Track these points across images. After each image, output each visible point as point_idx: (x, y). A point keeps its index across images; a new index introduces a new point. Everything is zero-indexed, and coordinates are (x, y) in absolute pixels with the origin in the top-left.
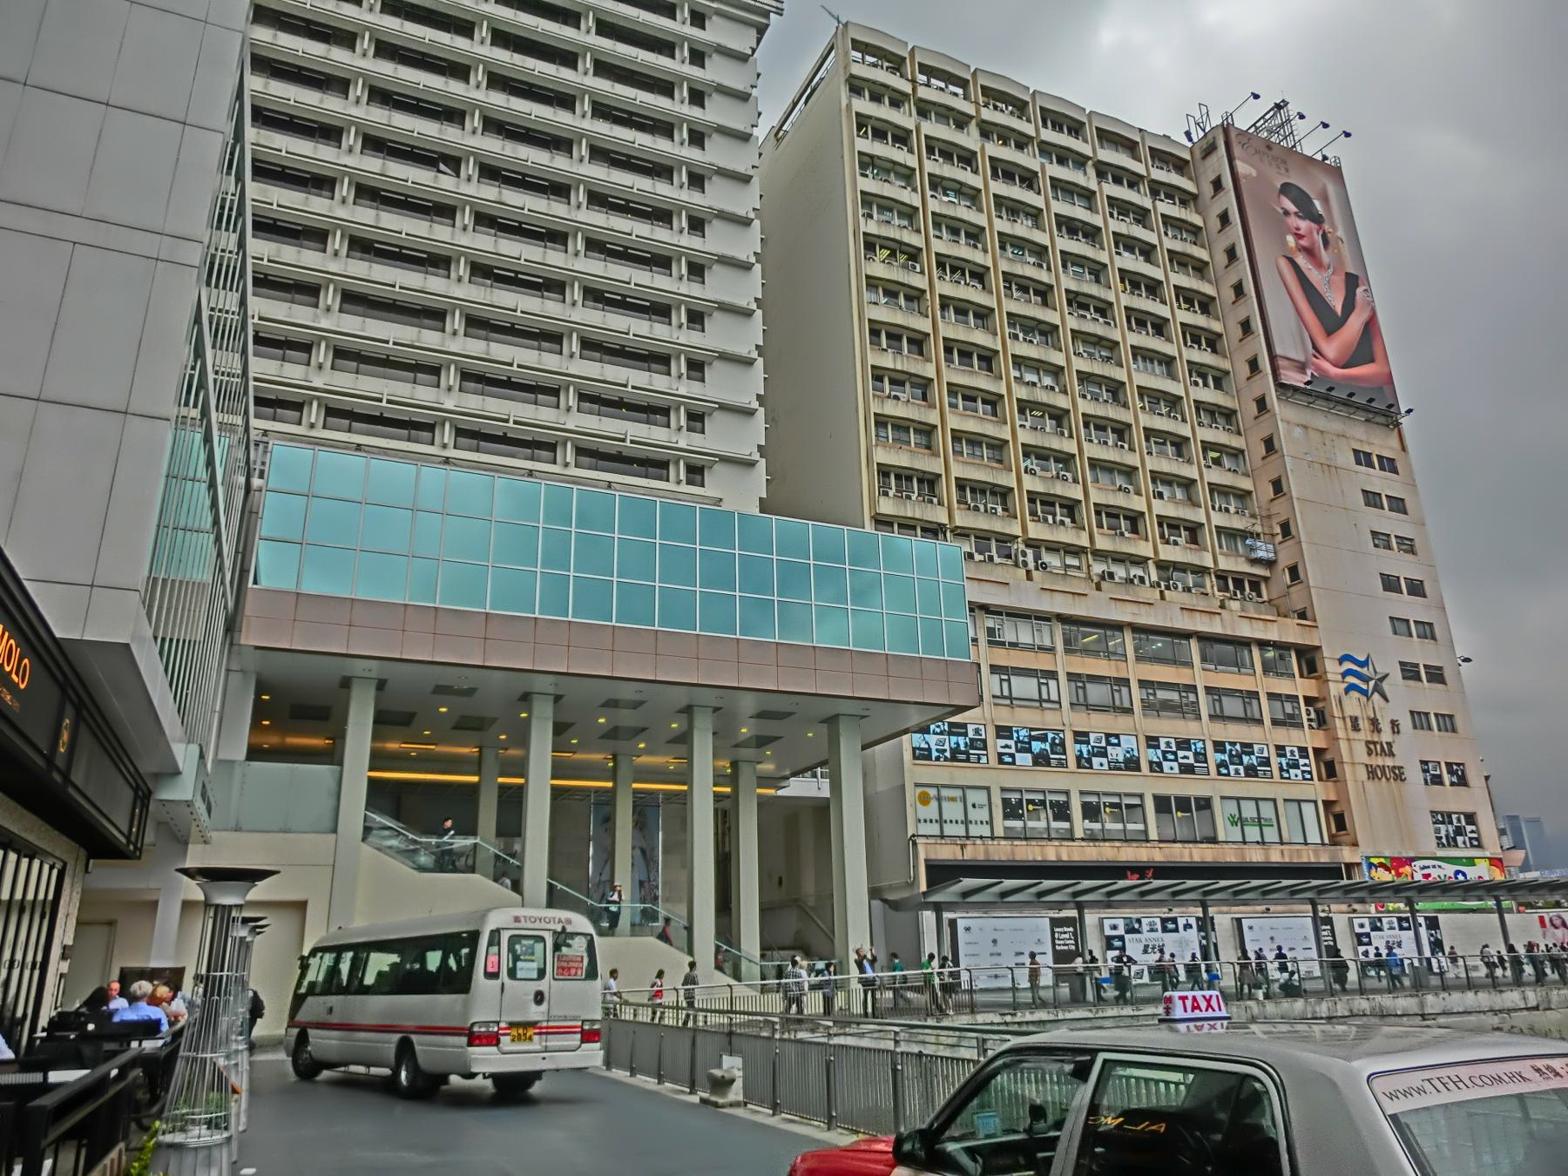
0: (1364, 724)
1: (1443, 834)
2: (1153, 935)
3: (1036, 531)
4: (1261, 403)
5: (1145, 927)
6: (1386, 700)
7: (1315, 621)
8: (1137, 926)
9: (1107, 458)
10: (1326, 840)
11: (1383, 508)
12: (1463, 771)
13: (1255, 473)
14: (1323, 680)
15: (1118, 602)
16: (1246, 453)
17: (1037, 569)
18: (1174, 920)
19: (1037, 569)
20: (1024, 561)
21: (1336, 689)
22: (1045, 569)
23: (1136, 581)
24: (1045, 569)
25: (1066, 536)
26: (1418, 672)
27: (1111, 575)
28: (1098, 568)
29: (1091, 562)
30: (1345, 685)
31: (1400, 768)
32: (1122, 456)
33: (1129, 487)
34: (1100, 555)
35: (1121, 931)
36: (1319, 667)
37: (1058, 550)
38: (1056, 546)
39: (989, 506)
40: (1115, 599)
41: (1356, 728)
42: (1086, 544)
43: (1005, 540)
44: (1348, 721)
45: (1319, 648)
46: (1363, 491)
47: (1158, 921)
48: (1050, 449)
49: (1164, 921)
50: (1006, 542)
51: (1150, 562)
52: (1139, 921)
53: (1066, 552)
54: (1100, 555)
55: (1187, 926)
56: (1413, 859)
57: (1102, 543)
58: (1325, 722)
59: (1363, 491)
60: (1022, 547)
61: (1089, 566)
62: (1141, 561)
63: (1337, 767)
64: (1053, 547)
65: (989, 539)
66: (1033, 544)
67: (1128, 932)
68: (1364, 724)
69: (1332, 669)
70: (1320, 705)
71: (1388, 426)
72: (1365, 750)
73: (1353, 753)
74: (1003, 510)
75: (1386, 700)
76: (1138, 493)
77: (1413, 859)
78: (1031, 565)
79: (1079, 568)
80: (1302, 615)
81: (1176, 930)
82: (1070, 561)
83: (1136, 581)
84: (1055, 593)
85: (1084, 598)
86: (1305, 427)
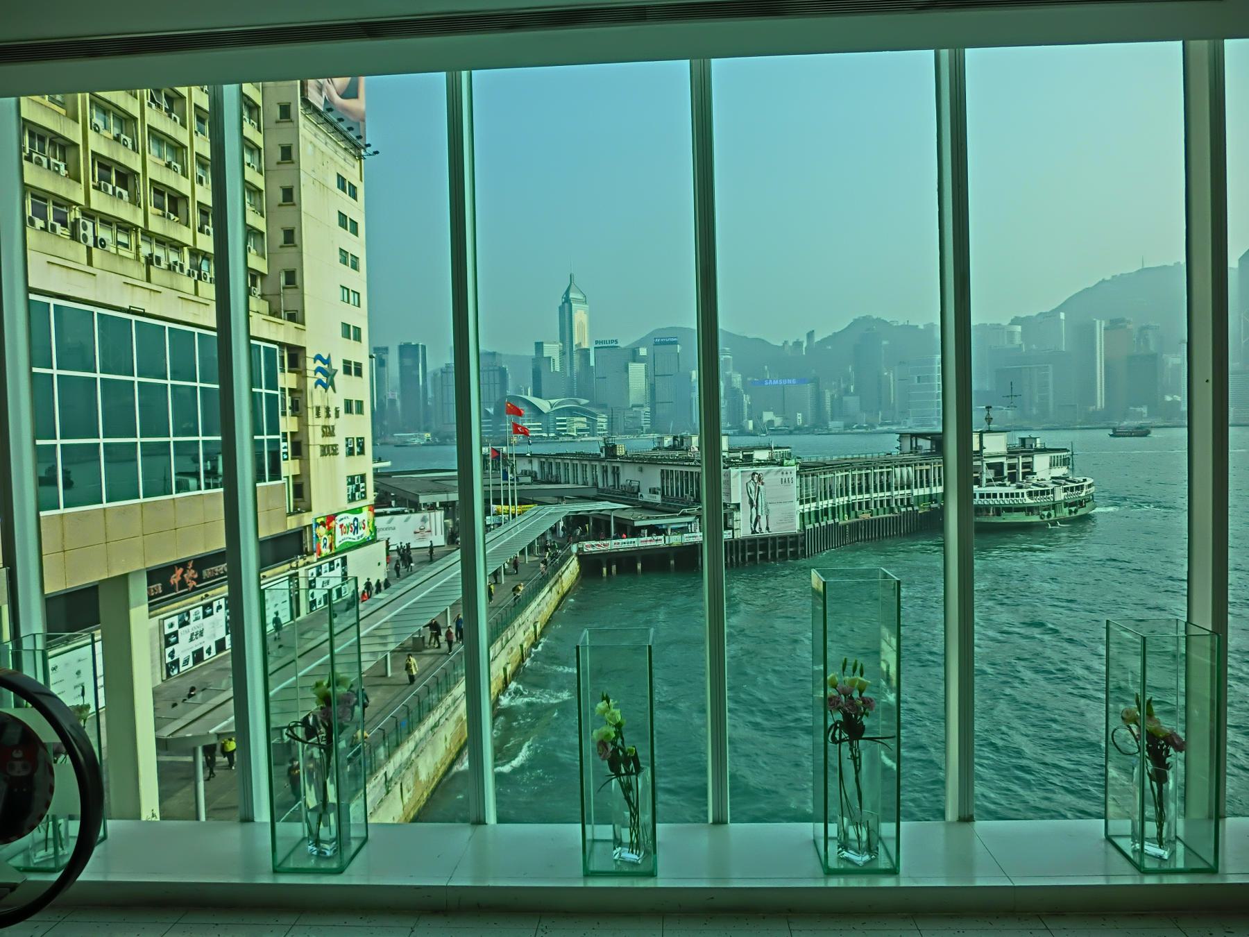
0: (323, 412)
1: (350, 491)
2: (198, 622)
3: (99, 202)
4: (285, 111)
5: (192, 617)
6: (335, 391)
7: (303, 324)
8: (186, 619)
9: (164, 131)
10: (292, 511)
11: (346, 229)
12: (363, 443)
13: (269, 173)
14: (302, 375)
15: (184, 301)
16: (263, 151)
17: (96, 246)
18: (210, 605)
19: (96, 246)
20: (84, 235)
21: (311, 382)
22: (103, 246)
23: (177, 268)
24: (103, 246)
25: (125, 211)
26: (350, 368)
27: (158, 260)
28: (145, 249)
29: (140, 243)
30: (316, 380)
31: (336, 445)
32: (176, 132)
33: (177, 165)
34: (148, 235)
35: (176, 628)
36: (301, 363)
37: (110, 224)
38: (109, 219)
39: (53, 160)
40: (182, 298)
41: (318, 415)
42: (141, 223)
43: (63, 203)
44: (315, 409)
45: (304, 348)
46: (339, 212)
47: (200, 609)
48: (117, 106)
49: (205, 607)
50: (62, 206)
51: (186, 249)
52: (188, 614)
53: (119, 227)
54: (148, 235)
55: (219, 607)
56: (336, 515)
57: (156, 226)
58: (297, 409)
59: (339, 212)
60: (79, 216)
61: (138, 247)
62: (177, 246)
63: (304, 448)
64: (107, 221)
65: (45, 200)
66: (89, 214)
67: (181, 626)
68: (323, 412)
69: (311, 365)
70: (297, 395)
71: (355, 157)
72: (321, 433)
73: (316, 438)
74: (66, 168)
75: (335, 391)
76: (184, 174)
77: (336, 515)
78: (91, 242)
79: (126, 246)
80: (292, 317)
81: (212, 614)
82: (122, 238)
83: (177, 268)
84: (135, 288)
85: (159, 294)
86: (315, 146)
